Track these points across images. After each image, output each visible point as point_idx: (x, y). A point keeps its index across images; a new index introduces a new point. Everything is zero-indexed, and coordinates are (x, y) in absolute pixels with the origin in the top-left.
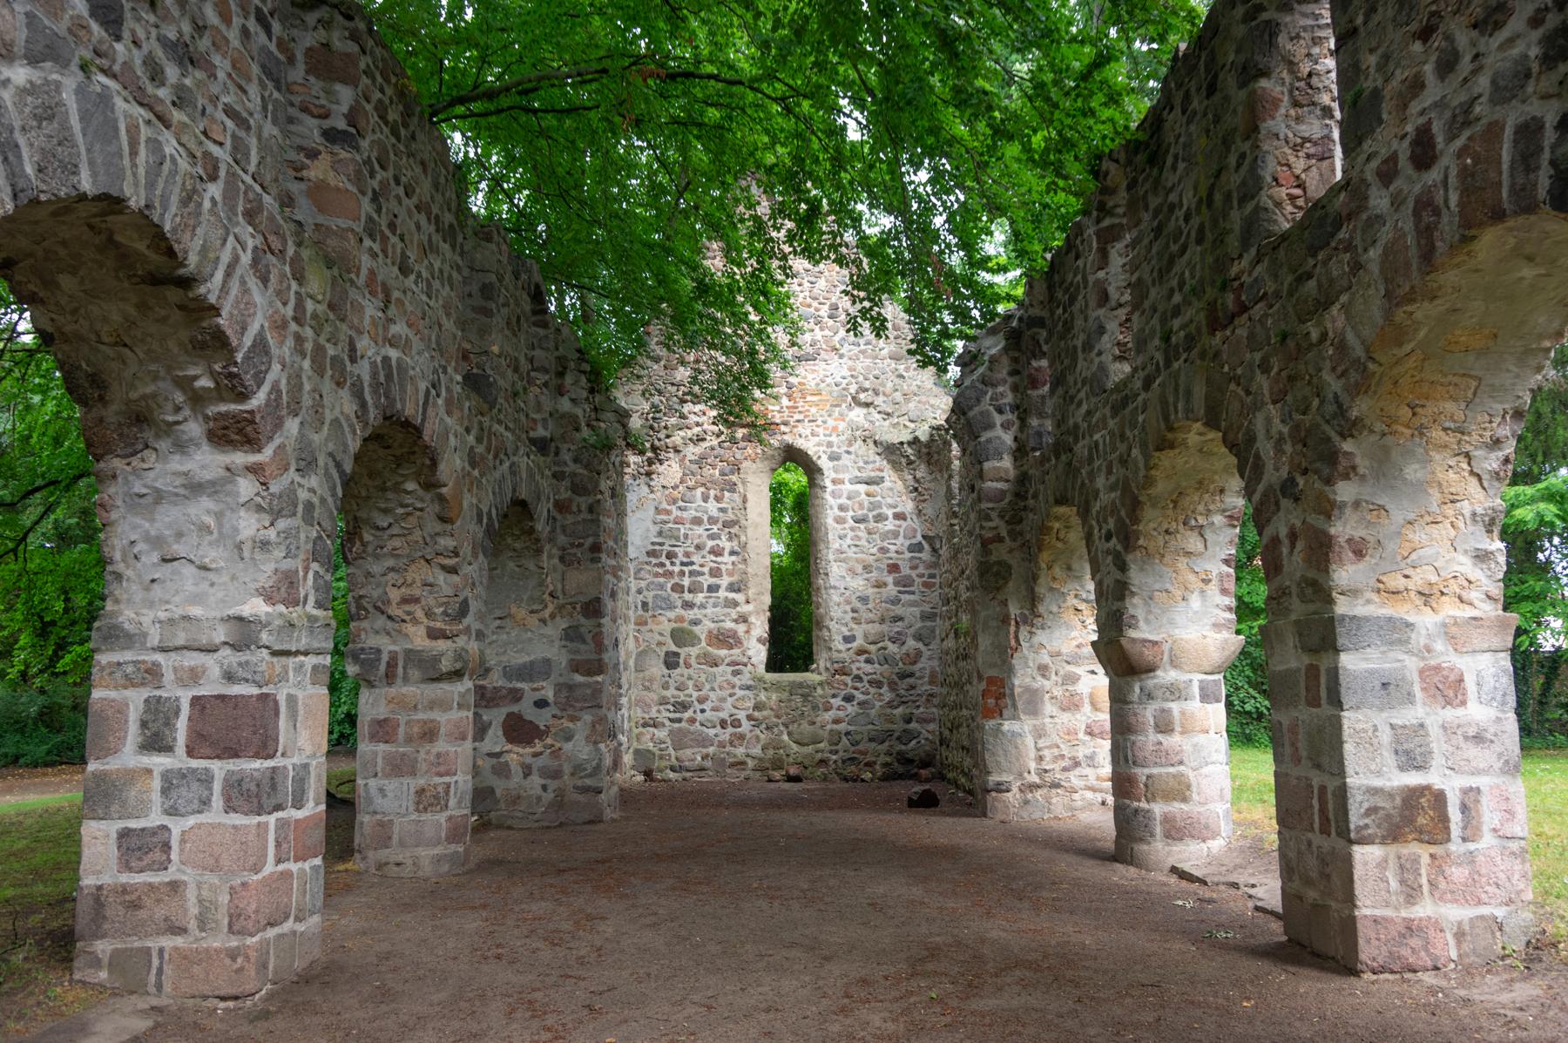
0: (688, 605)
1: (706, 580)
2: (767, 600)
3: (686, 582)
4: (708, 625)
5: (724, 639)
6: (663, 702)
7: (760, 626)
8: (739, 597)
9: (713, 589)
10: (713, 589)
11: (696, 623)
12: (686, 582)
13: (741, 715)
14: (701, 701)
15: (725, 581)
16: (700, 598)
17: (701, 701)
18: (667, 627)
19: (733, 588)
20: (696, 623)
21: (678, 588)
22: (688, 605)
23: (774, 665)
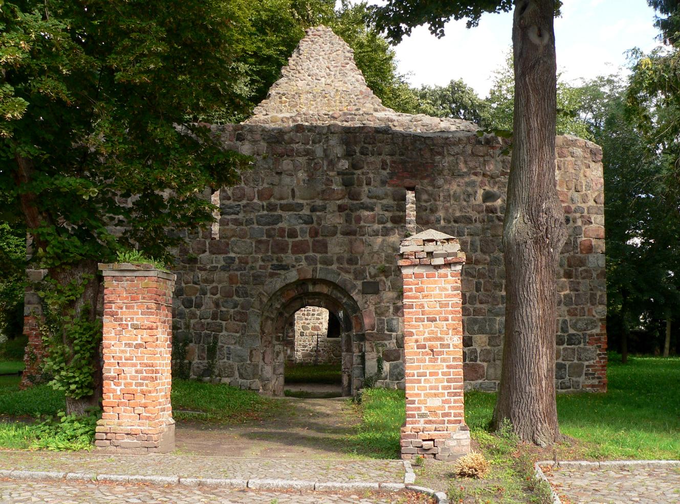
0: (306, 319)
1: (311, 312)
2: (328, 318)
3: (306, 313)
4: (312, 325)
5: (315, 328)
6: (300, 345)
7: (326, 325)
8: (320, 317)
9: (313, 315)
10: (313, 315)
11: (308, 324)
12: (306, 313)
13: (320, 349)
14: (310, 345)
15: (316, 313)
16: (309, 317)
17: (310, 345)
18: (301, 325)
19: (318, 315)
20: (308, 324)
21: (304, 314)
22: (306, 319)
23: (328, 336)
